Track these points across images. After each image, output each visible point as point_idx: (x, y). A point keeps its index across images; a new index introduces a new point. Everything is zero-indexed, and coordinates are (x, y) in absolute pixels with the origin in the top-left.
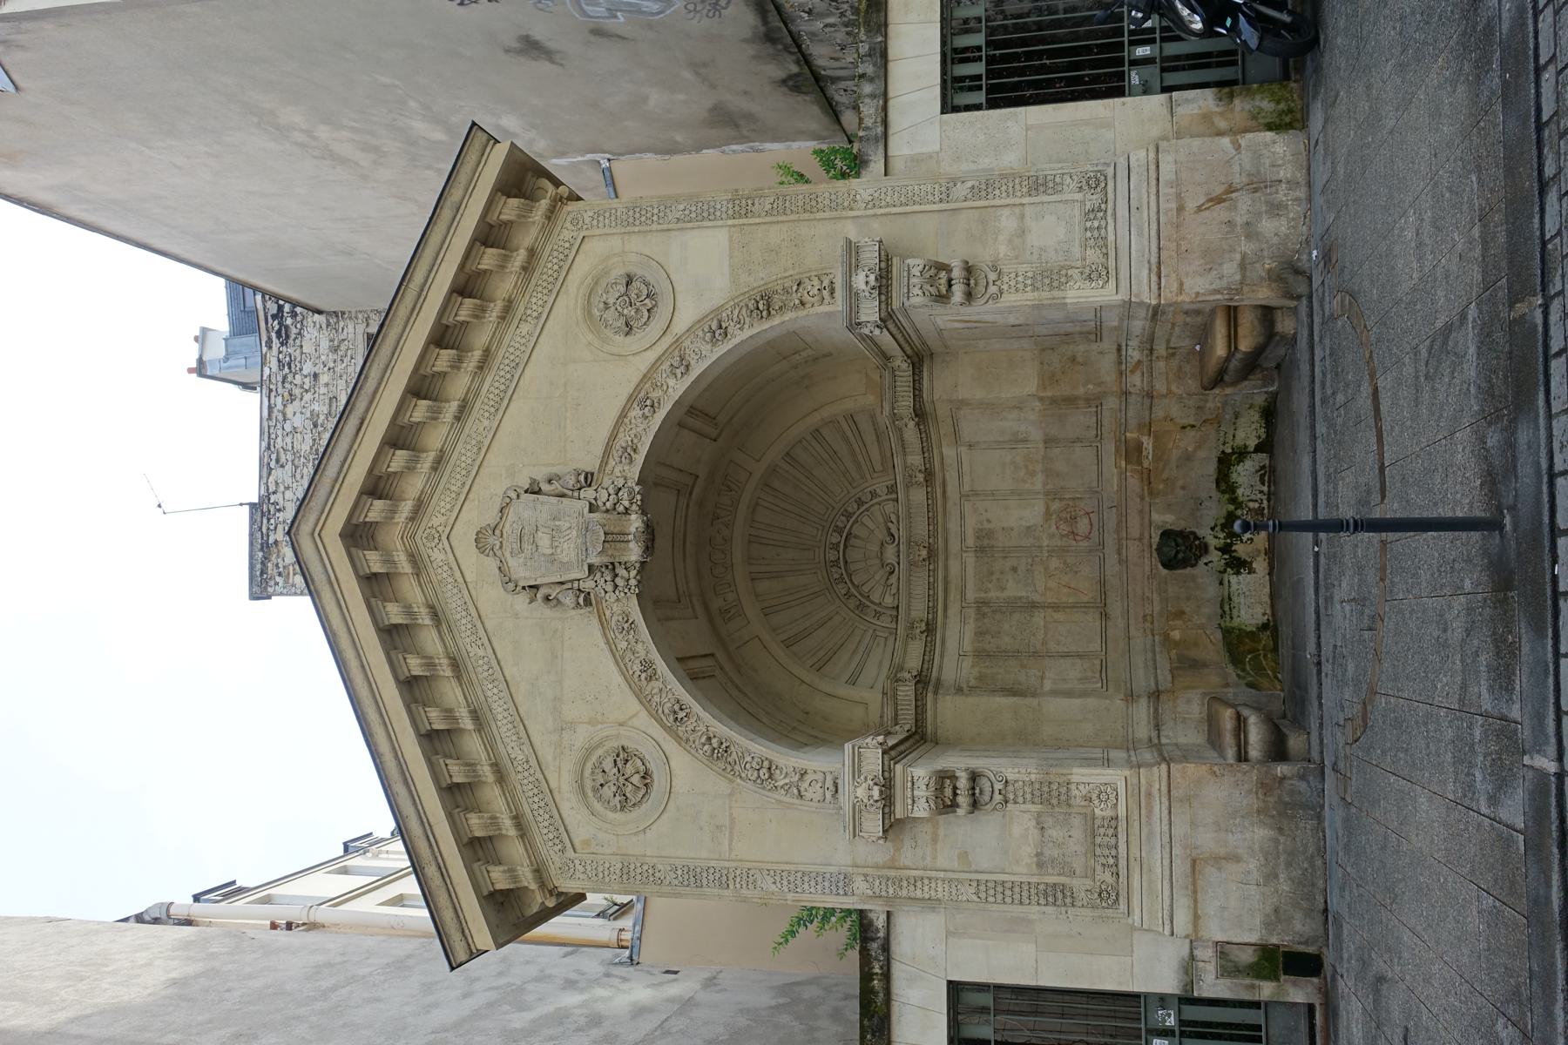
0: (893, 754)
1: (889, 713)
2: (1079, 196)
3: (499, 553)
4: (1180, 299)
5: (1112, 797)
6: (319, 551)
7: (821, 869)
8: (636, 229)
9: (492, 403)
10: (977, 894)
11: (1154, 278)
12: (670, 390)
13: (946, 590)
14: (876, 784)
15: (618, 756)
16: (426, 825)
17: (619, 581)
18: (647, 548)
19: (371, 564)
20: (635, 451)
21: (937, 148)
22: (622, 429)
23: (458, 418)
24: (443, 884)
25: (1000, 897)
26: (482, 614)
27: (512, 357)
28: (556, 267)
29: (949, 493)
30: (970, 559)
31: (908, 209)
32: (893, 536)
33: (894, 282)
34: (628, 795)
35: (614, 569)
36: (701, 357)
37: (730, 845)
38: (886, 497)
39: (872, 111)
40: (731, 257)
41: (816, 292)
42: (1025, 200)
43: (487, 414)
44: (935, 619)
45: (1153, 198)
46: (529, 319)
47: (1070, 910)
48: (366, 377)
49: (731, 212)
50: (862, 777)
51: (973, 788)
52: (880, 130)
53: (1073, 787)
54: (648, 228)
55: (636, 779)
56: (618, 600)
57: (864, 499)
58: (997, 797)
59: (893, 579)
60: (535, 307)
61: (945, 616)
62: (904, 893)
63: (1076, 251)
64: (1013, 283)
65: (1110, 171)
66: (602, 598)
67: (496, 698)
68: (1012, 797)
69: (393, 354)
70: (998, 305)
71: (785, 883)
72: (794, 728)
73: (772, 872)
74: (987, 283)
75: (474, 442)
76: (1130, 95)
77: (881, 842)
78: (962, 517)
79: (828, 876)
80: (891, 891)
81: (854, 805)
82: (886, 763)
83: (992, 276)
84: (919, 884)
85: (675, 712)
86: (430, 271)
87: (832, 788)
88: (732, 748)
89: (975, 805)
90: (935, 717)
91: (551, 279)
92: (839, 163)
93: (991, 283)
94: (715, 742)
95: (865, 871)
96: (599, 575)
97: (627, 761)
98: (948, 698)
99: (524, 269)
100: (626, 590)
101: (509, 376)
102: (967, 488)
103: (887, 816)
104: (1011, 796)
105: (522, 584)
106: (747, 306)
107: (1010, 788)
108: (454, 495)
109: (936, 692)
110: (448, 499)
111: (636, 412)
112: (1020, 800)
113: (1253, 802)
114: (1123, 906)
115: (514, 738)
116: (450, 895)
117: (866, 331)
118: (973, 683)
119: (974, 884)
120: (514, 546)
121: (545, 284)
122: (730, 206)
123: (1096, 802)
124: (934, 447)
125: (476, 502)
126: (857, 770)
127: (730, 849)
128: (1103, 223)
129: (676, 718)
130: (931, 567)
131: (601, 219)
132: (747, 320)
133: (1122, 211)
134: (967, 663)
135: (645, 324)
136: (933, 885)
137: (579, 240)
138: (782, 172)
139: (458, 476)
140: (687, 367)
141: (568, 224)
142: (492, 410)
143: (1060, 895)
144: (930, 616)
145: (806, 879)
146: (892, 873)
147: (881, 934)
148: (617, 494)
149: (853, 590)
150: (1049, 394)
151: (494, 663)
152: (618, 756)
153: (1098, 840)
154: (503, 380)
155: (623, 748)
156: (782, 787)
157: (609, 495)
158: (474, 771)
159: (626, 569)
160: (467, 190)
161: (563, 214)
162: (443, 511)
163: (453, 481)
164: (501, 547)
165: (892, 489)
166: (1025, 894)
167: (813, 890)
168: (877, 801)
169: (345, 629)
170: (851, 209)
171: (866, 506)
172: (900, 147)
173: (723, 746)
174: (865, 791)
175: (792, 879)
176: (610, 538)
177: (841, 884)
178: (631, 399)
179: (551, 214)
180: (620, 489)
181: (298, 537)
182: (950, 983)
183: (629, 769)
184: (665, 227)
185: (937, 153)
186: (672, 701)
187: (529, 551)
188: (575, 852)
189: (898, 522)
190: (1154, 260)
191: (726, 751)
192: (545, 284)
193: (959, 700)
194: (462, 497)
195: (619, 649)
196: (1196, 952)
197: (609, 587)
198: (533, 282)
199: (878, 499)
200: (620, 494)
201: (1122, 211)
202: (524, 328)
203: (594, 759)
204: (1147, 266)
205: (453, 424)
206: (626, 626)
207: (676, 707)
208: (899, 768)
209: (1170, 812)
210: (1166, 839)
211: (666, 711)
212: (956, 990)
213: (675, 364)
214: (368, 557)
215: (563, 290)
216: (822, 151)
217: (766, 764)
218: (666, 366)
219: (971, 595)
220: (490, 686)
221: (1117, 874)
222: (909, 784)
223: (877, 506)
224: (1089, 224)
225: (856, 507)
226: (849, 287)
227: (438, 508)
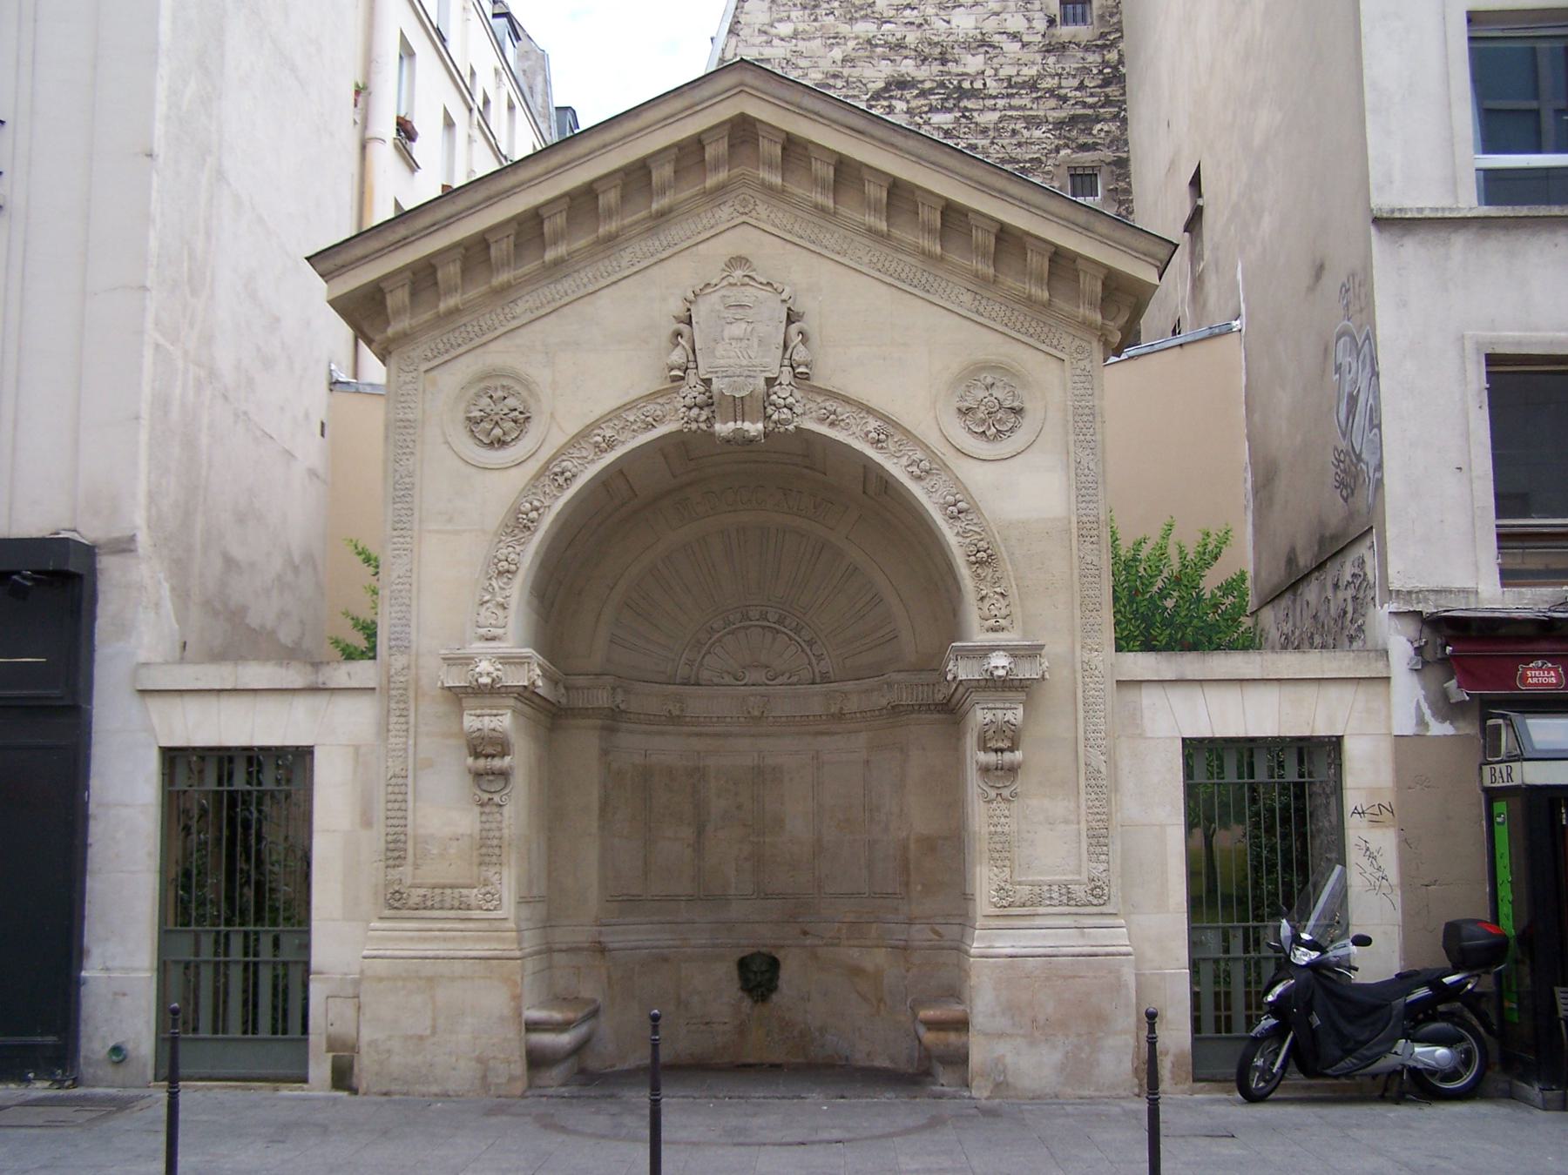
0: (526, 695)
2: (1084, 877)
3: (725, 283)
5: (489, 905)
7: (413, 624)
8: (1070, 418)
9: (887, 264)
10: (394, 776)
12: (895, 460)
13: (716, 735)
14: (493, 680)
15: (521, 413)
17: (695, 411)
18: (729, 441)
19: (714, 145)
25: (392, 797)
27: (936, 285)
31: (1080, 706)
34: (482, 424)
35: (708, 405)
36: (929, 492)
38: (817, 671)
41: (993, 613)
42: (1084, 826)
43: (875, 260)
46: (977, 303)
47: (382, 864)
49: (1085, 519)
51: (493, 773)
53: (497, 869)
54: (1071, 431)
55: (497, 432)
58: (486, 796)
60: (989, 308)
61: (690, 735)
67: (578, 282)
70: (976, 797)
71: (400, 587)
73: (408, 574)
74: (999, 788)
77: (439, 684)
79: (407, 629)
80: (393, 693)
83: (1006, 793)
85: (563, 473)
88: (528, 533)
89: (478, 775)
92: (1228, 601)
94: (534, 515)
95: (413, 667)
96: (702, 390)
99: (1029, 297)
100: (686, 419)
103: (463, 690)
104: (487, 810)
105: (692, 308)
106: (982, 540)
107: (495, 809)
108: (789, 227)
109: (603, 728)
111: (873, 424)
114: (388, 913)
119: (403, 773)
121: (1013, 318)
123: (483, 891)
126: (506, 660)
129: (554, 474)
131: (1083, 379)
136: (401, 733)
137: (1059, 355)
138: (1221, 534)
140: (919, 478)
143: (396, 854)
144: (688, 719)
145: (404, 608)
146: (411, 694)
148: (785, 406)
149: (717, 635)
150: (912, 846)
151: (614, 278)
154: (911, 276)
155: (529, 418)
156: (490, 585)
157: (784, 399)
158: (503, 265)
159: (708, 418)
160: (1108, 239)
162: (772, 216)
163: (804, 225)
167: (393, 615)
168: (477, 681)
170: (1083, 647)
173: (530, 524)
174: (485, 669)
175: (403, 593)
180: (791, 409)
183: (508, 425)
184: (1072, 448)
186: (574, 470)
188: (426, 371)
191: (525, 527)
192: (1013, 318)
194: (788, 237)
197: (688, 401)
198: (1017, 306)
200: (785, 410)
202: (967, 298)
205: (865, 225)
206: (650, 419)
207: (568, 474)
211: (564, 464)
213: (921, 465)
214: (721, 141)
216: (1244, 581)
217: (513, 567)
218: (919, 455)
220: (590, 275)
221: (417, 909)
222: (495, 712)
224: (1055, 888)
227: (775, 209)
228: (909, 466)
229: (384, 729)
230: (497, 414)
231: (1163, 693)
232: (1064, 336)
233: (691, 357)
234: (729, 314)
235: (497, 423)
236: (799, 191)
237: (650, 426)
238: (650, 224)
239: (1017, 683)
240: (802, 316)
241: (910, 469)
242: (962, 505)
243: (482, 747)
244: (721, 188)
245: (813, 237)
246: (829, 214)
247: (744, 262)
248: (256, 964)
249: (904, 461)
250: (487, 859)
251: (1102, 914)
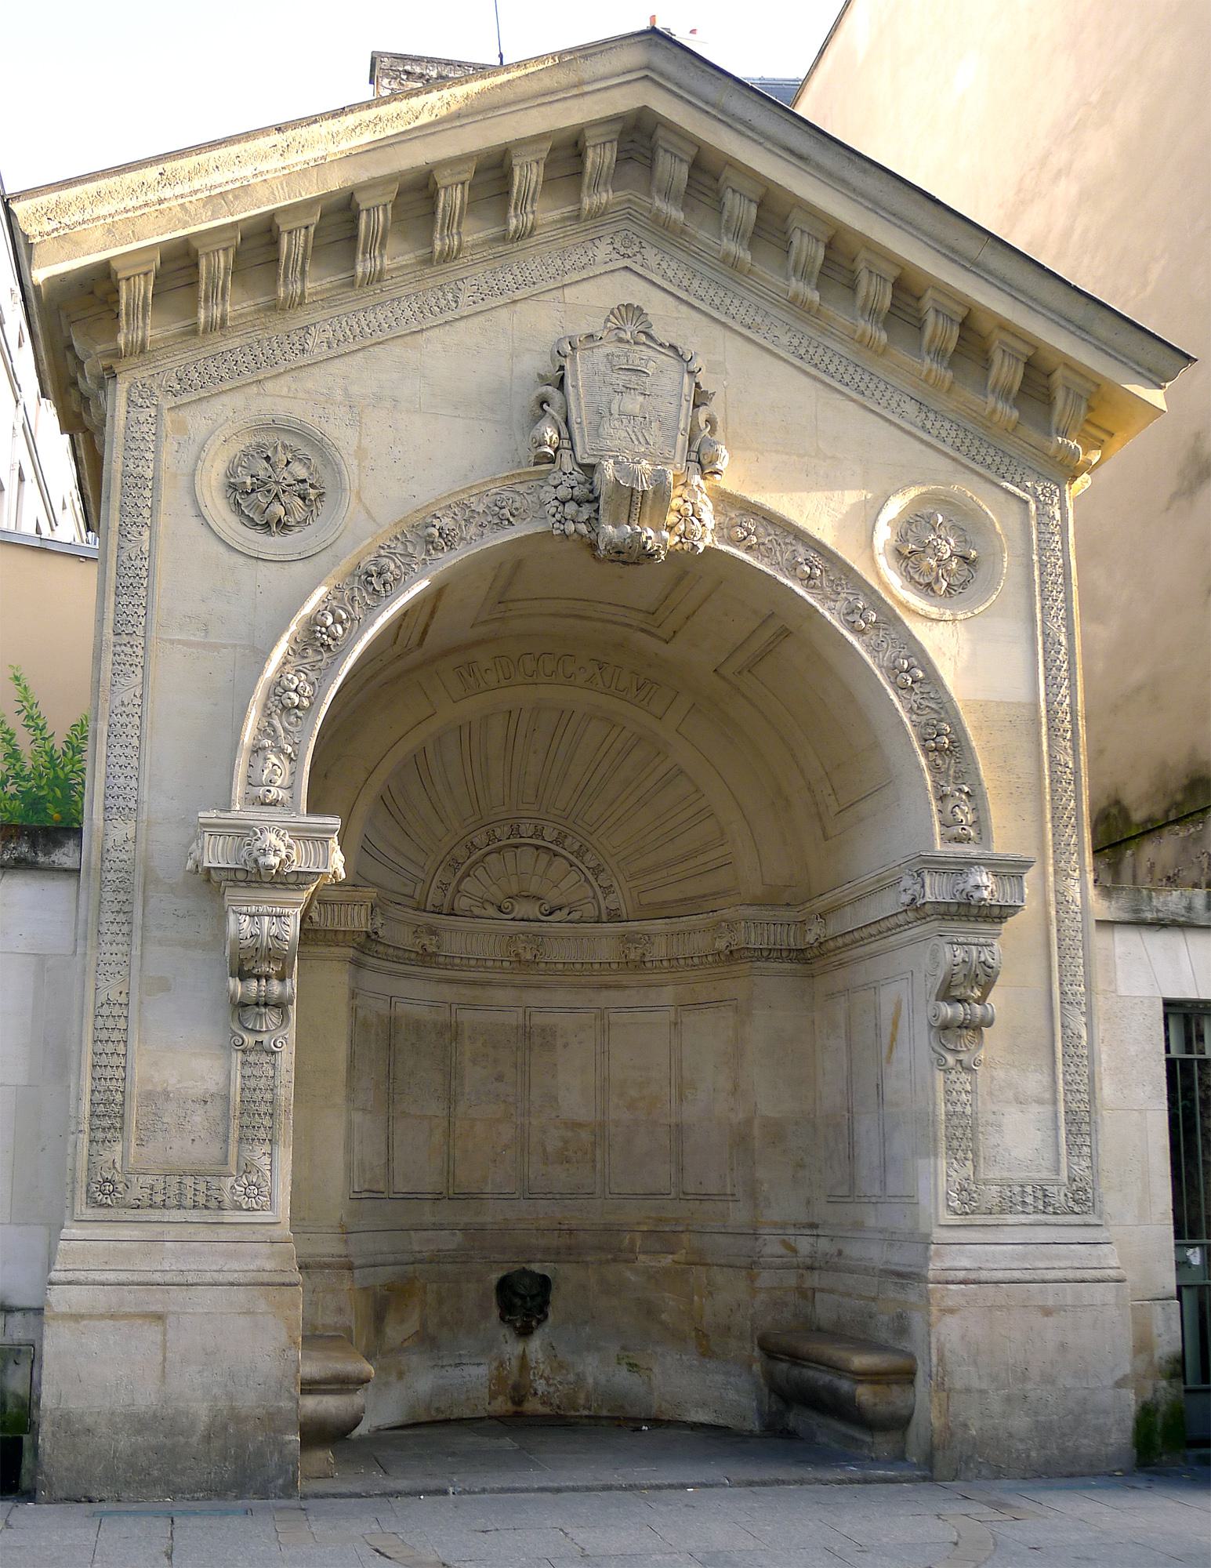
2: (1064, 1176)
4: (934, 1310)
9: (812, 351)
11: (961, 1275)
13: (474, 983)
15: (311, 486)
17: (571, 508)
21: (1122, 991)
28: (989, 460)
29: (605, 993)
30: (514, 1018)
32: (550, 914)
33: (971, 925)
35: (588, 501)
38: (603, 907)
39: (1172, 907)
40: (998, 704)
43: (796, 342)
44: (438, 966)
45: (1060, 1274)
46: (923, 415)
52: (1149, 916)
56: (542, 504)
57: (602, 876)
59: (491, 911)
60: (938, 424)
61: (440, 981)
62: (109, 896)
63: (994, 1173)
64: (958, 1087)
65: (1091, 1219)
66: (545, 480)
68: (251, 1059)
76: (1176, 1245)
77: (190, 864)
78: (573, 1010)
80: (110, 876)
81: (250, 827)
84: (121, 918)
85: (380, 574)
97: (303, 499)
100: (558, 516)
101: (847, 378)
102: (614, 1017)
103: (231, 875)
104: (251, 1059)
107: (265, 1058)
108: (686, 283)
112: (248, 1071)
113: (248, 1401)
114: (90, 1213)
117: (907, 882)
119: (123, 999)
125: (675, 315)
127: (172, 642)
128: (1030, 1209)
132: (923, 719)
133: (1043, 1234)
134: (382, 1007)
135: (912, 578)
136: (120, 938)
142: (802, 351)
143: (107, 1122)
144: (441, 960)
146: (138, 880)
147: (41, 859)
151: (449, 316)
152: (311, 486)
153: (189, 1181)
156: (270, 724)
162: (664, 265)
165: (614, 917)
168: (256, 861)
171: (591, 878)
172: (1127, 945)
175: (129, 730)
177: (121, 802)
185: (1115, 991)
190: (984, 1275)
191: (322, 645)
193: (343, 992)
196: (18, 1316)
197: (562, 492)
198: (969, 426)
201: (1043, 1234)
203: (305, 451)
204: (976, 1265)
209: (232, 1284)
210: (191, 1278)
215: (959, 467)
219: (466, 1017)
220: (415, 306)
221: (138, 1207)
223: (591, 895)
224: (1029, 1189)
225: (592, 864)
226: (971, 863)
227: (667, 258)
228: (848, 614)
230: (277, 483)
231: (1139, 937)
233: (564, 434)
234: (620, 378)
236: (703, 235)
237: (503, 522)
239: (996, 911)
241: (849, 618)
243: (252, 964)
244: (599, 213)
246: (740, 272)
250: (249, 1133)
251: (1085, 1225)
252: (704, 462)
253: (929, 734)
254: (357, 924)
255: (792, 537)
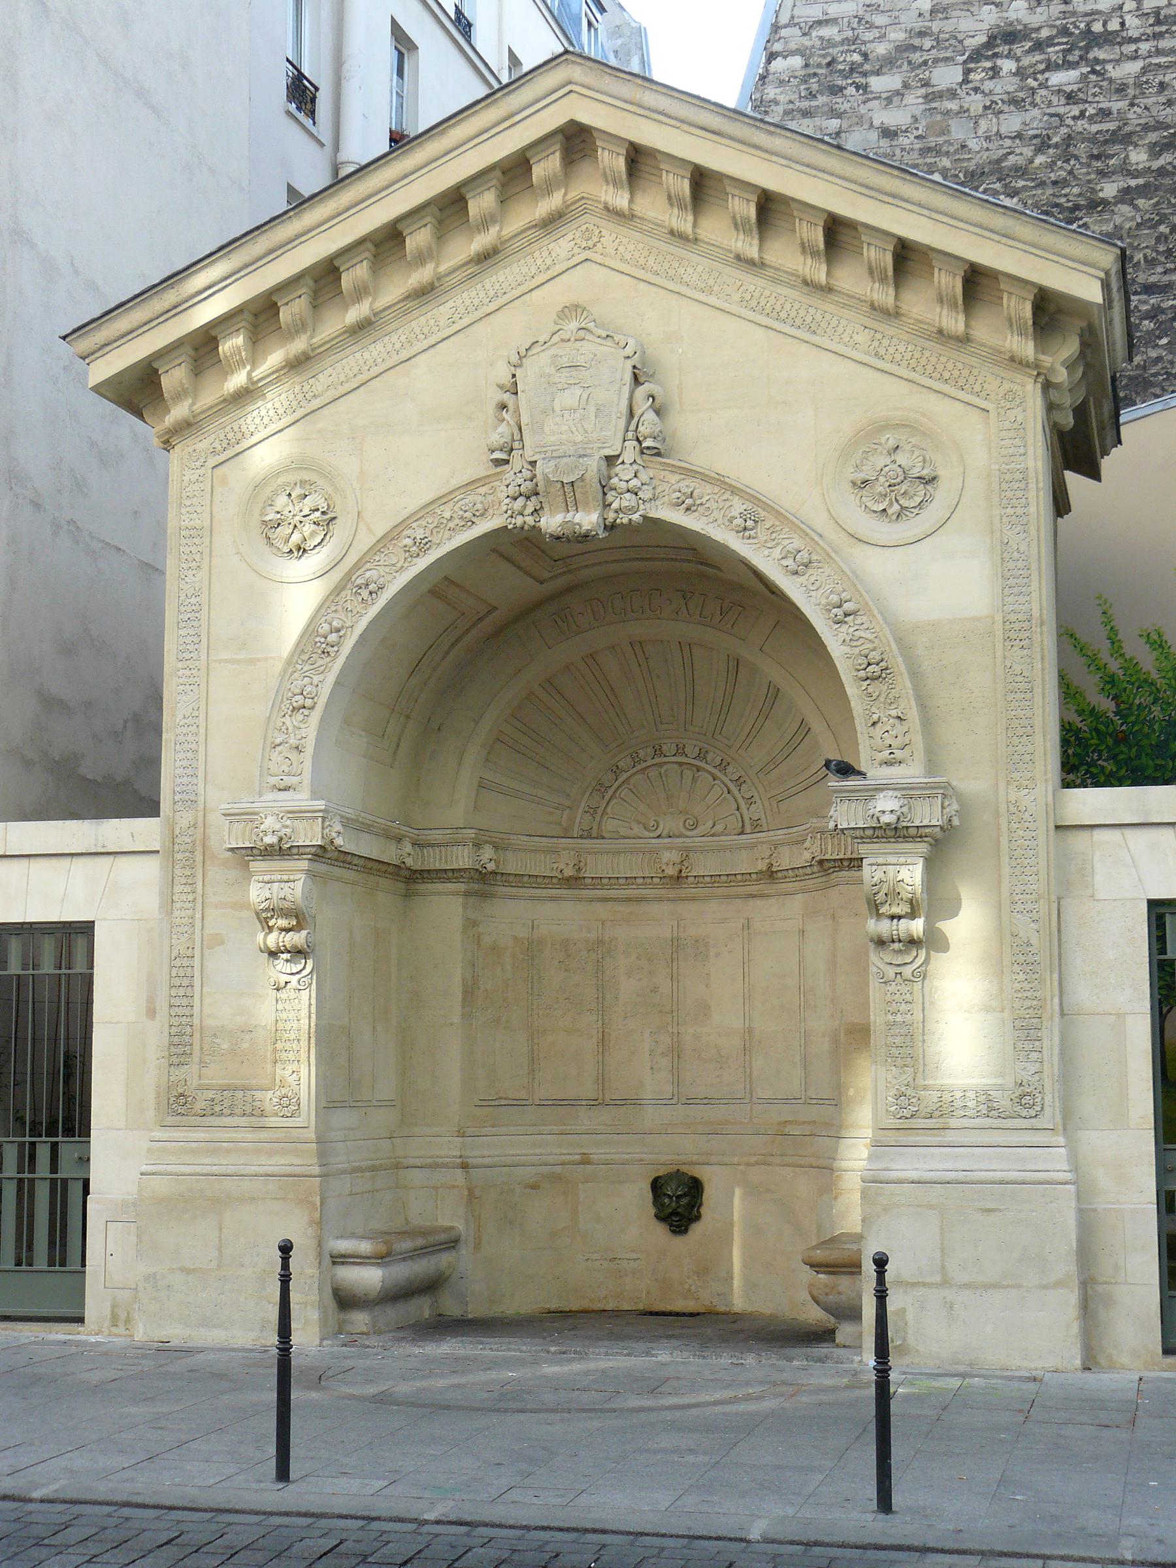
1: (436, 836)
3: (556, 338)
6: (548, 95)
8: (995, 486)
10: (179, 956)
12: (766, 552)
14: (281, 839)
16: (224, 284)
17: (521, 501)
18: (558, 538)
19: (542, 163)
20: (688, 509)
22: (716, 489)
23: (738, 257)
24: (156, 313)
25: (177, 982)
26: (491, 316)
28: (946, 375)
37: (226, 661)
41: (888, 742)
43: (747, 296)
46: (876, 343)
48: (772, 133)
49: (1013, 617)
50: (289, 822)
53: (295, 1067)
62: (178, 872)
69: (808, 166)
71: (185, 730)
72: (408, 717)
75: (711, 282)
82: (308, 850)
83: (907, 971)
84: (188, 889)
86: (920, 205)
87: (282, 785)
88: (329, 659)
90: (439, 894)
91: (930, 369)
93: (899, 970)
95: (200, 824)
98: (460, 909)
99: (940, 332)
103: (249, 852)
105: (519, 372)
106: (874, 649)
107: (293, 995)
108: (642, 261)
109: (467, 894)
110: (637, 255)
111: (738, 506)
114: (170, 1120)
115: (342, 378)
116: (145, 324)
118: (487, 940)
119: (189, 953)
120: (565, 359)
121: (923, 361)
122: (1021, 617)
124: (802, 883)
126: (296, 814)
130: (656, 880)
132: (857, 651)
137: (983, 404)
139: (666, 265)
140: (795, 573)
141: (1007, 386)
143: (180, 1050)
145: (190, 755)
146: (199, 857)
151: (432, 341)
158: (297, 332)
161: (1019, 378)
162: (622, 249)
163: (660, 258)
164: (563, 340)
166: (180, 1011)
167: (178, 763)
169: (450, 146)
170: (1008, 783)
173: (329, 649)
174: (270, 829)
175: (189, 738)
176: (568, 489)
177: (185, 797)
178: (754, 499)
179: (1015, 362)
180: (636, 494)
181: (564, 65)
182: (93, 922)
187: (558, 380)
188: (213, 468)
189: (712, 835)
191: (323, 652)
194: (640, 274)
195: (442, 508)
197: (512, 490)
198: (928, 344)
199: (743, 806)
200: (628, 495)
202: (863, 337)
205: (730, 251)
206: (467, 515)
207: (372, 587)
208: (304, 865)
211: (368, 574)
212: (86, 929)
217: (308, 703)
218: (797, 543)
220: (403, 338)
222: (285, 877)
229: (168, 902)
232: (990, 378)
233: (516, 432)
234: (563, 377)
235: (295, 526)
238: (472, 269)
239: (913, 832)
240: (652, 376)
241: (785, 562)
242: (847, 606)
245: (671, 272)
247: (579, 310)
248: (32, 1181)
249: (777, 553)
252: (641, 439)
253: (860, 665)
254: (461, 863)
255: (729, 493)
